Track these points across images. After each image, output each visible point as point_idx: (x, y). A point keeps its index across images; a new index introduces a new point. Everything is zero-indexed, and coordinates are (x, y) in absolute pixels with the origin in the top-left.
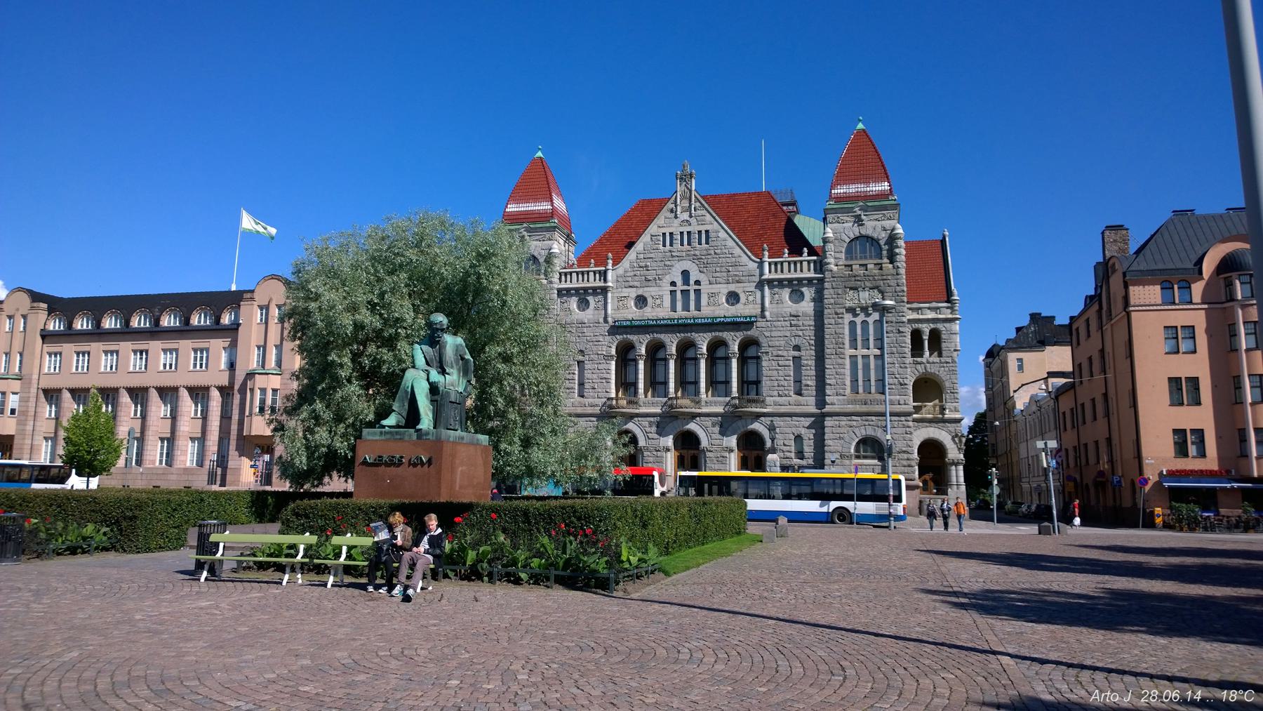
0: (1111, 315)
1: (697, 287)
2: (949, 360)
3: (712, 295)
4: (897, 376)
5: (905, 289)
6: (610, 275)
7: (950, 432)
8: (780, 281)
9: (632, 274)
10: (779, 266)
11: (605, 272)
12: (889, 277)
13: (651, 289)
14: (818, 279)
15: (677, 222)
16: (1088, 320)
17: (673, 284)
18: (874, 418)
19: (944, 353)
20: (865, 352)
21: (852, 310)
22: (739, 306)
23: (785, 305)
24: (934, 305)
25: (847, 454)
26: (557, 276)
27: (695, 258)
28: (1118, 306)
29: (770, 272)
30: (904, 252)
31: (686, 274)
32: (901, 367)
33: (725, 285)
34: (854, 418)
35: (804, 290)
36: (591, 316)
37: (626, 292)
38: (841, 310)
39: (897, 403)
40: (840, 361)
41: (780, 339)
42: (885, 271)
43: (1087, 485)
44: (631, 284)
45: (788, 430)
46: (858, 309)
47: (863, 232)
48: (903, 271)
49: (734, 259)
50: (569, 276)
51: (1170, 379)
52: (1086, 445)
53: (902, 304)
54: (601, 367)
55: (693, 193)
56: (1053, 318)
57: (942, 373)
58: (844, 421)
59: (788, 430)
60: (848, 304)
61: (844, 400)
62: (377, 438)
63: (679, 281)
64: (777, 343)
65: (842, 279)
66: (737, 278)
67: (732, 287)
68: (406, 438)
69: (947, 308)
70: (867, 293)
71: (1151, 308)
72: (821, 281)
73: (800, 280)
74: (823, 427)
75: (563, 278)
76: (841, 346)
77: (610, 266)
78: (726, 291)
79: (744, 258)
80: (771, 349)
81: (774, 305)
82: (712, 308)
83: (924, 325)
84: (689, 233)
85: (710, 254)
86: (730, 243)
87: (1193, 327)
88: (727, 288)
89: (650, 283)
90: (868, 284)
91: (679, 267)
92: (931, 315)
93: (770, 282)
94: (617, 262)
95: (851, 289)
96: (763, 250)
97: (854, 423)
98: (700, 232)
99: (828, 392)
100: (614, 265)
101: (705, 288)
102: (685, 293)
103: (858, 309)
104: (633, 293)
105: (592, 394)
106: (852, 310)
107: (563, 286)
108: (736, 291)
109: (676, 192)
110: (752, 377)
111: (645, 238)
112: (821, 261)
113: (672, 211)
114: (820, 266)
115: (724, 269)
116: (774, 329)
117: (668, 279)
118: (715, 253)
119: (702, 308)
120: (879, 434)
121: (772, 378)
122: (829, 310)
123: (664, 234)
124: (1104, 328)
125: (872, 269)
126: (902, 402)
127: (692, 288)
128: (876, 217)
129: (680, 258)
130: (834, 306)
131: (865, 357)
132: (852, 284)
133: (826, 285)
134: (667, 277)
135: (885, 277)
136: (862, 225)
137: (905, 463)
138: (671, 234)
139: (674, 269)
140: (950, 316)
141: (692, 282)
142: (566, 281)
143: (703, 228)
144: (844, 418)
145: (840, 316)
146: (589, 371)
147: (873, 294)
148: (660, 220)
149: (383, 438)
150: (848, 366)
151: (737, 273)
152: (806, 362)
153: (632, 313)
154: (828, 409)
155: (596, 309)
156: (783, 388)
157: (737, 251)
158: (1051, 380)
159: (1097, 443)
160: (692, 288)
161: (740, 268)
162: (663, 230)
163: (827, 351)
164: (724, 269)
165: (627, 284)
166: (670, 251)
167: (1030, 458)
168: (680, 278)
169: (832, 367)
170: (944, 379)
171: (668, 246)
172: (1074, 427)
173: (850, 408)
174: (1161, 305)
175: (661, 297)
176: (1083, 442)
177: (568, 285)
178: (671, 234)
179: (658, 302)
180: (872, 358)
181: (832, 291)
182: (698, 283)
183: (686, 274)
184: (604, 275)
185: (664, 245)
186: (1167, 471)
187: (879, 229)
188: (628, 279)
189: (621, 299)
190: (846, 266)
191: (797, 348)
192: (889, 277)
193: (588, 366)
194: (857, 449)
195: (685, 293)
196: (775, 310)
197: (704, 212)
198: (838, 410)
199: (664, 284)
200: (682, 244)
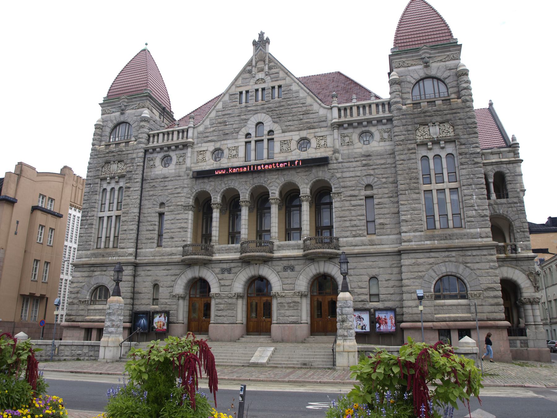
2: (515, 200)
3: (283, 142)
7: (523, 271)
8: (350, 124)
9: (212, 129)
10: (348, 111)
12: (459, 111)
13: (228, 142)
15: (253, 81)
17: (248, 135)
19: (510, 194)
20: (440, 186)
23: (356, 146)
27: (269, 111)
33: (297, 133)
35: (373, 129)
36: (173, 171)
38: (413, 146)
40: (415, 196)
41: (351, 179)
44: (210, 139)
45: (363, 271)
54: (178, 217)
57: (511, 214)
58: (422, 259)
59: (363, 271)
60: (419, 139)
61: (421, 236)
63: (252, 132)
64: (349, 184)
66: (309, 125)
67: (304, 134)
69: (509, 152)
70: (437, 128)
73: (369, 122)
75: (151, 139)
78: (297, 138)
79: (316, 107)
80: (342, 190)
81: (345, 147)
82: (285, 154)
83: (489, 168)
88: (299, 135)
89: (227, 137)
90: (439, 119)
91: (254, 120)
95: (422, 124)
101: (278, 136)
103: (430, 144)
104: (211, 147)
105: (169, 243)
108: (308, 136)
110: (325, 222)
115: (295, 118)
116: (345, 170)
117: (244, 131)
118: (289, 105)
119: (275, 155)
120: (461, 271)
121: (345, 219)
128: (440, 59)
129: (256, 112)
130: (405, 142)
134: (243, 129)
139: (249, 122)
143: (276, 84)
145: (411, 151)
146: (169, 222)
152: (380, 200)
153: (209, 164)
156: (355, 228)
157: (309, 100)
160: (265, 138)
161: (311, 116)
162: (240, 89)
164: (295, 118)
165: (206, 139)
166: (246, 107)
168: (254, 129)
169: (406, 202)
175: (236, 148)
179: (234, 153)
182: (271, 132)
188: (207, 134)
189: (200, 152)
191: (369, 186)
192: (459, 111)
193: (166, 218)
200: (256, 100)
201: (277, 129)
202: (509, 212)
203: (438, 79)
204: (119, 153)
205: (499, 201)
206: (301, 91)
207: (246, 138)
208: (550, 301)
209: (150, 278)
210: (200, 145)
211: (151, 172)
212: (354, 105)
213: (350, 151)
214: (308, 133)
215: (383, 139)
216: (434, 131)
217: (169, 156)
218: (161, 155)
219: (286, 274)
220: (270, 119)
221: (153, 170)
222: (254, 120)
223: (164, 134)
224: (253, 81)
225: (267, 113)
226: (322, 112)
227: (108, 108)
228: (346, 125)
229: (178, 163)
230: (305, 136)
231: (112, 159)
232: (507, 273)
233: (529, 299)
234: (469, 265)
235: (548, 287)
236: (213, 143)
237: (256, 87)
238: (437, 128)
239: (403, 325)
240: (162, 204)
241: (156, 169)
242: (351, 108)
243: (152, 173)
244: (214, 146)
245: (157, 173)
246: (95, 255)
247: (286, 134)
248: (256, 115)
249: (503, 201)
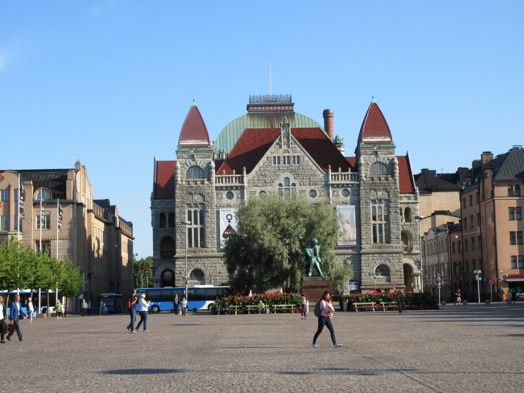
0: (484, 198)
4: (396, 234)
5: (399, 191)
6: (245, 179)
7: (414, 260)
8: (338, 185)
10: (336, 177)
11: (242, 178)
12: (392, 184)
13: (269, 187)
14: (357, 185)
15: (281, 151)
16: (471, 197)
17: (280, 185)
18: (385, 255)
20: (380, 222)
21: (374, 201)
22: (317, 198)
23: (340, 197)
24: (407, 195)
25: (372, 273)
26: (214, 179)
27: (292, 171)
28: (488, 196)
29: (332, 180)
30: (398, 172)
32: (397, 230)
34: (375, 255)
37: (254, 189)
39: (395, 247)
40: (368, 227)
42: (389, 181)
43: (467, 283)
44: (257, 184)
46: (377, 200)
47: (378, 160)
48: (398, 182)
49: (313, 172)
50: (220, 179)
51: (511, 232)
52: (467, 262)
53: (398, 198)
55: (290, 134)
56: (435, 171)
57: (411, 230)
61: (370, 246)
62: (309, 280)
65: (369, 185)
67: (313, 187)
68: (318, 280)
70: (381, 192)
71: (504, 198)
72: (359, 185)
74: (361, 260)
76: (369, 219)
77: (245, 174)
81: (334, 198)
83: (403, 205)
84: (288, 157)
85: (300, 169)
86: (310, 163)
87: (521, 207)
88: (310, 188)
91: (283, 175)
92: (405, 200)
93: (333, 185)
94: (248, 172)
95: (373, 190)
97: (376, 258)
98: (294, 156)
99: (363, 242)
100: (247, 173)
101: (298, 187)
103: (377, 200)
106: (374, 201)
107: (218, 185)
109: (280, 134)
111: (264, 159)
112: (358, 175)
113: (278, 144)
114: (358, 177)
117: (277, 182)
118: (303, 168)
120: (388, 263)
122: (363, 201)
123: (275, 157)
124: (481, 204)
125: (383, 180)
126: (398, 247)
128: (384, 152)
131: (380, 225)
132: (374, 187)
133: (362, 188)
135: (389, 184)
136: (378, 156)
137: (399, 276)
138: (279, 157)
139: (280, 177)
140: (415, 201)
141: (291, 184)
142: (219, 182)
143: (296, 155)
144: (371, 255)
145: (368, 204)
147: (384, 193)
148: (272, 149)
149: (311, 280)
150: (372, 229)
151: (315, 180)
154: (363, 251)
155: (237, 198)
157: (314, 168)
158: (438, 217)
159: (474, 261)
162: (274, 155)
163: (362, 222)
165: (255, 184)
167: (427, 267)
170: (412, 233)
171: (277, 165)
172: (460, 251)
173: (374, 250)
174: (507, 197)
176: (466, 259)
177: (220, 185)
178: (279, 157)
180: (383, 226)
181: (364, 191)
182: (294, 185)
183: (287, 179)
184: (241, 180)
185: (275, 163)
186: (508, 275)
187: (386, 159)
190: (370, 178)
192: (392, 184)
194: (376, 271)
196: (335, 200)
197: (296, 146)
198: (368, 252)
199: (275, 185)
200: (285, 163)
201: (297, 183)
202: (411, 230)
203: (383, 164)
204: (198, 188)
205: (406, 223)
207: (279, 186)
208: (440, 264)
210: (251, 188)
211: (220, 201)
212: (340, 174)
213: (337, 200)
214: (314, 188)
216: (380, 193)
218: (226, 192)
220: (293, 176)
221: (221, 200)
222: (283, 175)
223: (226, 178)
227: (183, 154)
228: (335, 186)
230: (313, 189)
231: (194, 192)
232: (407, 261)
233: (416, 274)
234: (391, 261)
235: (440, 253)
236: (259, 188)
237: (284, 155)
238: (381, 192)
239: (361, 287)
241: (223, 200)
242: (338, 175)
243: (221, 202)
244: (260, 189)
245: (224, 202)
246: (188, 251)
247: (303, 187)
248: (284, 173)
249: (409, 223)
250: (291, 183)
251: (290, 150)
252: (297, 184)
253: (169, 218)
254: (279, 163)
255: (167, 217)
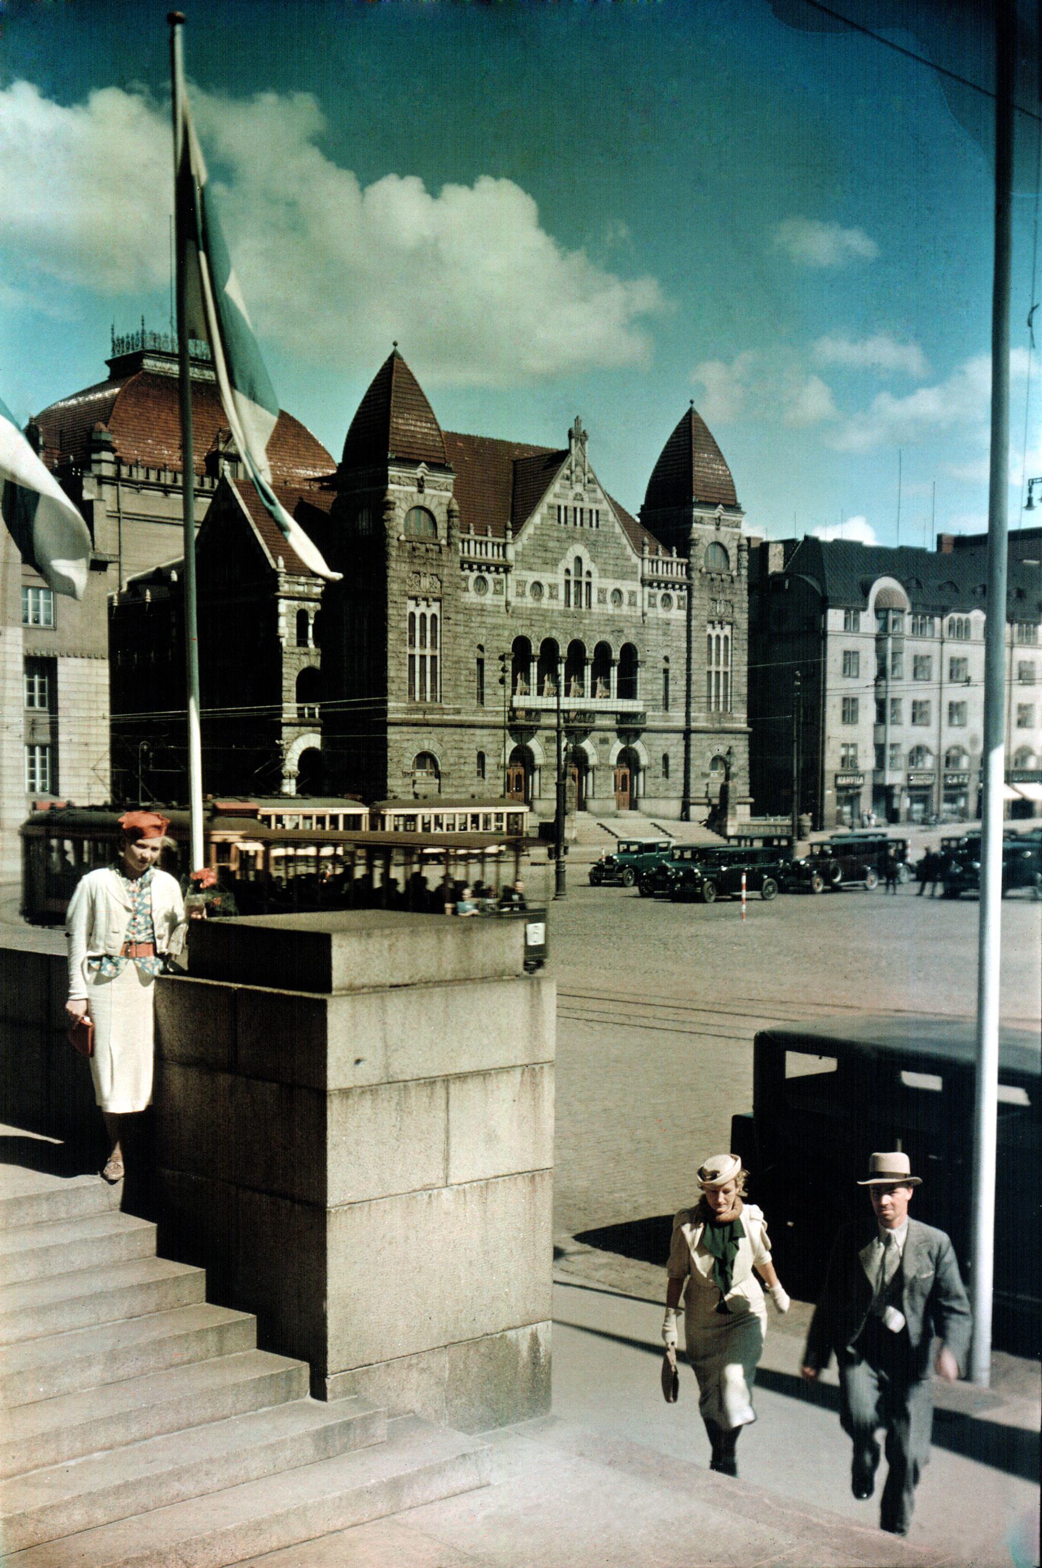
1: (588, 580)
3: (602, 591)
11: (505, 546)
17: (568, 571)
31: (579, 560)
59: (660, 749)
63: (572, 567)
81: (651, 609)
96: (644, 545)
101: (596, 582)
102: (578, 583)
104: (531, 577)
113: (568, 478)
127: (584, 579)
138: (566, 508)
141: (584, 573)
143: (594, 507)
183: (579, 560)
195: (578, 583)
206: (617, 525)
209: (473, 746)
215: (679, 608)
217: (483, 579)
218: (476, 574)
219: (600, 747)
224: (571, 494)
225: (586, 546)
226: (635, 559)
229: (496, 592)
240: (481, 648)
246: (410, 711)
250: (585, 568)
251: (586, 496)
252: (595, 574)
253: (314, 625)
254: (566, 522)
255: (311, 621)
